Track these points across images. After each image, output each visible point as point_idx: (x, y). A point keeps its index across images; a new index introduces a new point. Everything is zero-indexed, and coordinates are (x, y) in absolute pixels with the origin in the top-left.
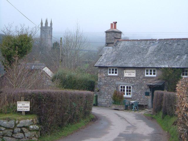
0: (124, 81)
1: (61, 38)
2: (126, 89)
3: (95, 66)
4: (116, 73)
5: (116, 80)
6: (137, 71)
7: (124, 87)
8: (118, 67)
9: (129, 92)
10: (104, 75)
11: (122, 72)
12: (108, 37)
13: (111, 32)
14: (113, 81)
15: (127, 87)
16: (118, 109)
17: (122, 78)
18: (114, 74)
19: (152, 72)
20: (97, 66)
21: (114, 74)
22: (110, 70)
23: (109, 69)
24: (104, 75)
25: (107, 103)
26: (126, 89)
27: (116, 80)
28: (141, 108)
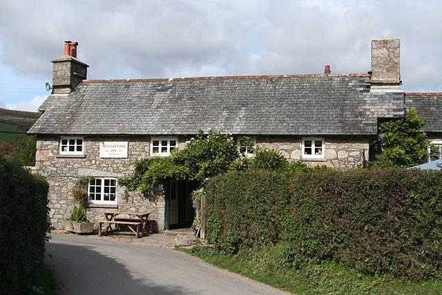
0: (99, 167)
1: (72, 48)
2: (103, 186)
3: (30, 134)
4: (79, 149)
5: (80, 166)
6: (131, 143)
7: (99, 182)
8: (323, 136)
9: (95, 193)
10: (51, 155)
11: (94, 147)
12: (59, 73)
13: (65, 61)
14: (73, 169)
15: (107, 182)
16: (84, 237)
17: (93, 162)
18: (76, 153)
19: (313, 147)
20: (33, 134)
21: (76, 153)
22: (156, 143)
23: (162, 142)
24: (51, 155)
25: (58, 219)
26: (103, 186)
27: (80, 166)
28: (125, 233)
